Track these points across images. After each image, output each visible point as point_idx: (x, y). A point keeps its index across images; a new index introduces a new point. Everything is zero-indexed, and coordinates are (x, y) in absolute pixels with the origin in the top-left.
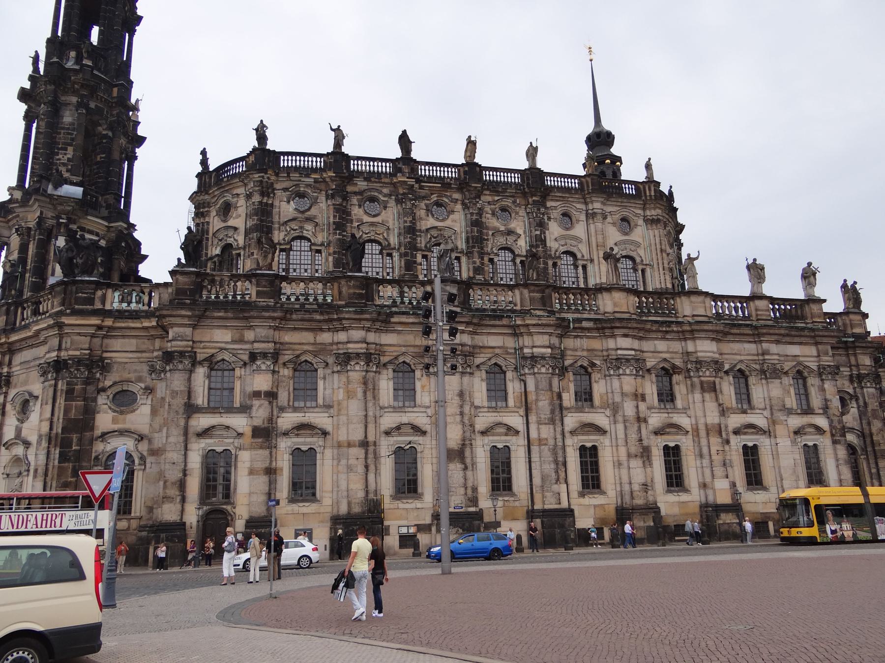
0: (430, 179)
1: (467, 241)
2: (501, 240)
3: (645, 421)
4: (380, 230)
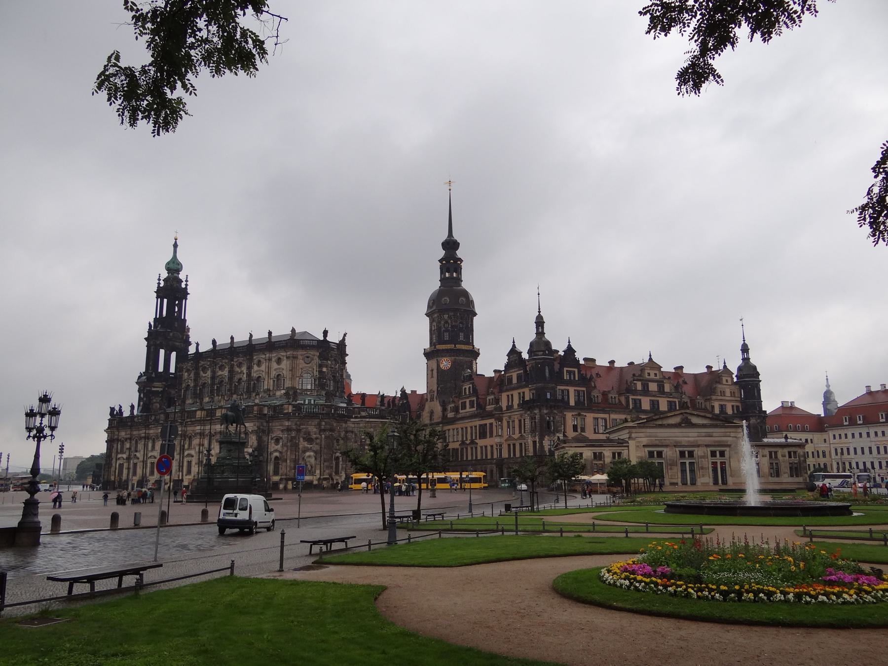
2: (238, 376)
3: (202, 452)
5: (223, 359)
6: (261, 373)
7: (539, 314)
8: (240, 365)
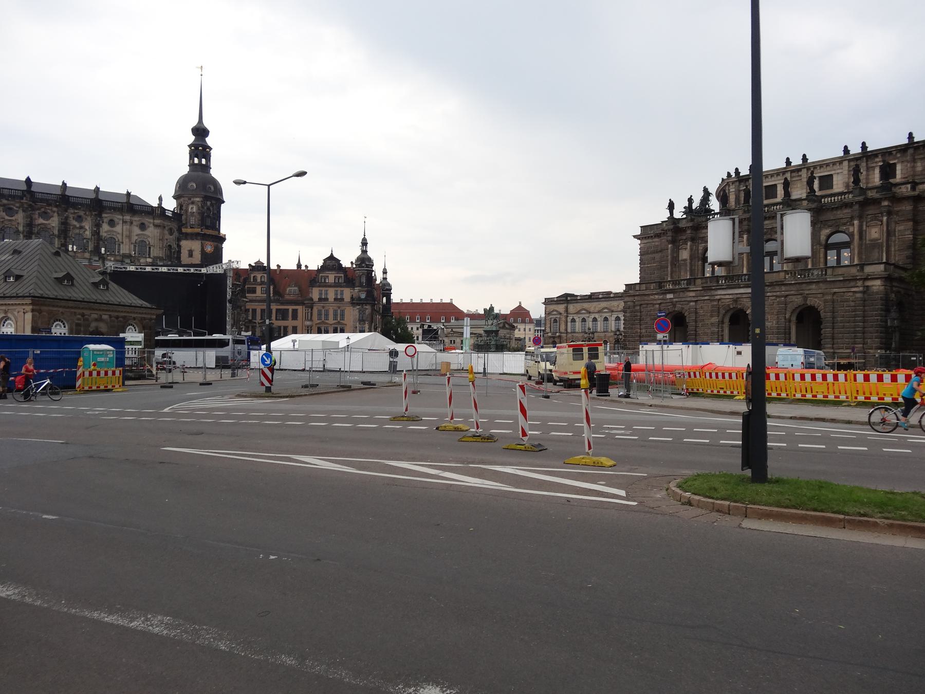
0: (42, 200)
1: (59, 231)
2: (77, 231)
4: (14, 223)
5: (49, 205)
6: (114, 234)
7: (364, 237)
8: (79, 219)
